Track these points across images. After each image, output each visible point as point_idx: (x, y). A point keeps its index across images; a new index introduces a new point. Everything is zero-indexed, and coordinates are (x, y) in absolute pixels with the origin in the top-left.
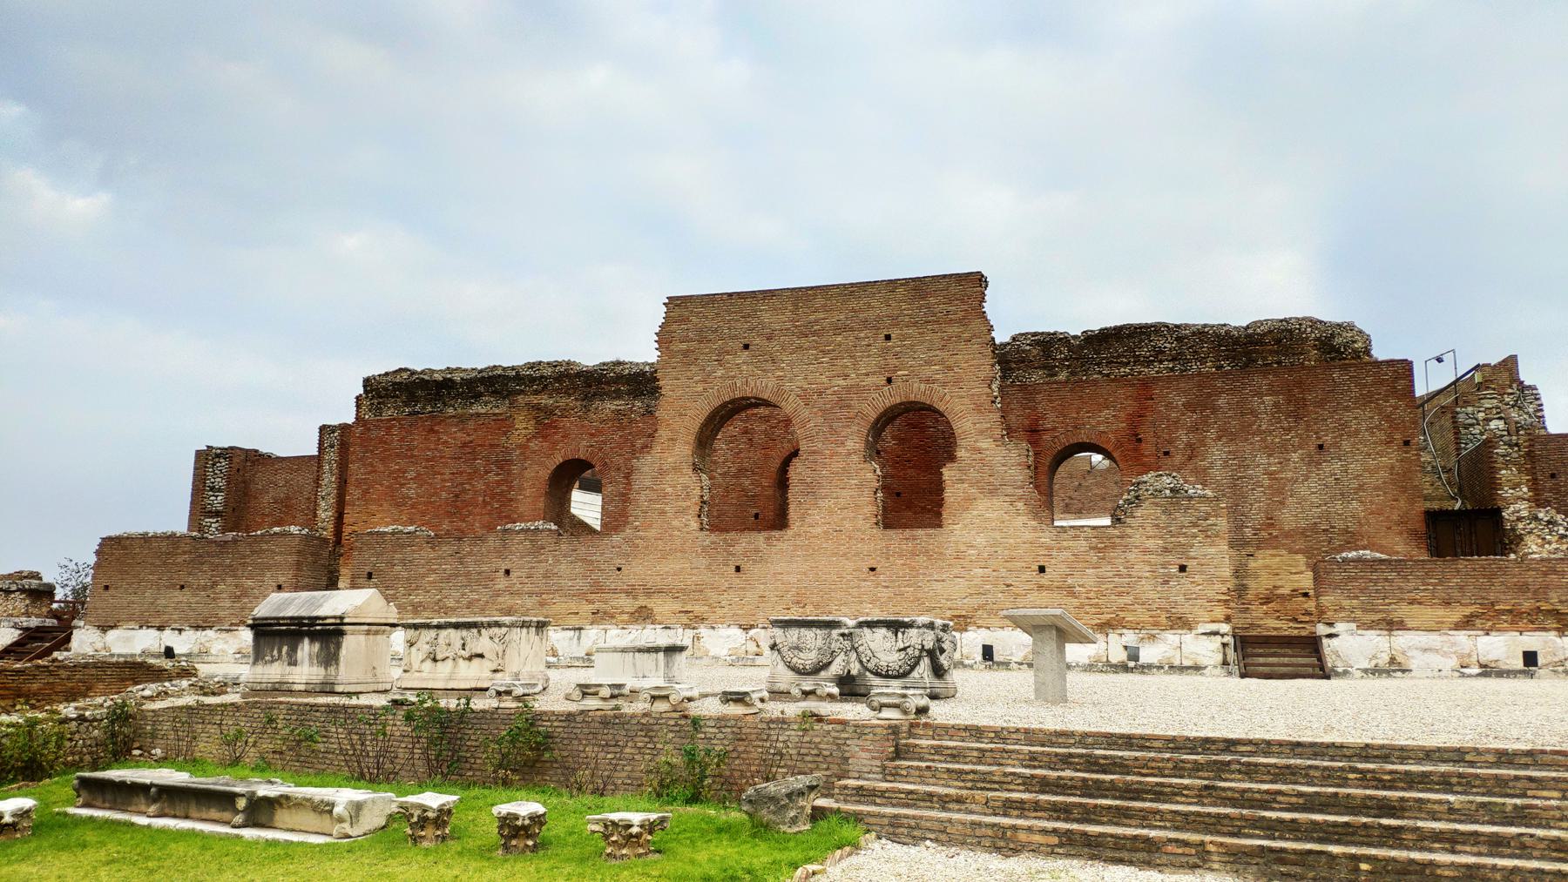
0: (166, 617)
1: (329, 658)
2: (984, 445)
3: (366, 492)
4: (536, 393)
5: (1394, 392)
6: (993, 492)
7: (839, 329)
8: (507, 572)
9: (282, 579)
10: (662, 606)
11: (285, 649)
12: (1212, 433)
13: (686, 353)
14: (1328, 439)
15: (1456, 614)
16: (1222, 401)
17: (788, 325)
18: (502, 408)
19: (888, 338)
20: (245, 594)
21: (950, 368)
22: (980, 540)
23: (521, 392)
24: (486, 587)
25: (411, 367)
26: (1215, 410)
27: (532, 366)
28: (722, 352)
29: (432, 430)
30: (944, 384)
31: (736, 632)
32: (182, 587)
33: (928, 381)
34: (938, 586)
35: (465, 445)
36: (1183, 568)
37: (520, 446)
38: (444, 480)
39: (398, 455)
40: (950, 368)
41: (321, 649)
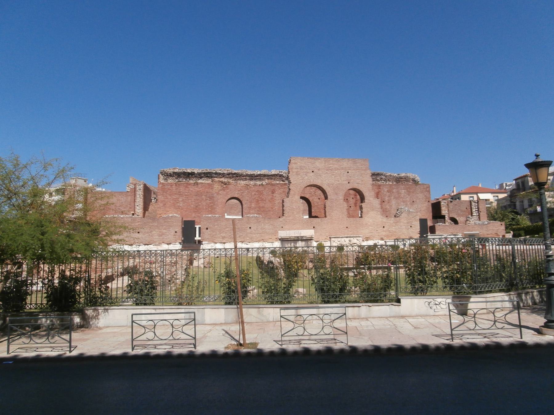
3: (165, 204)
4: (221, 178)
5: (426, 191)
6: (373, 210)
12: (392, 198)
13: (297, 172)
14: (414, 200)
16: (394, 191)
18: (209, 181)
20: (163, 234)
22: (371, 221)
23: (216, 177)
28: (307, 173)
29: (187, 187)
30: (362, 184)
35: (198, 191)
39: (176, 194)
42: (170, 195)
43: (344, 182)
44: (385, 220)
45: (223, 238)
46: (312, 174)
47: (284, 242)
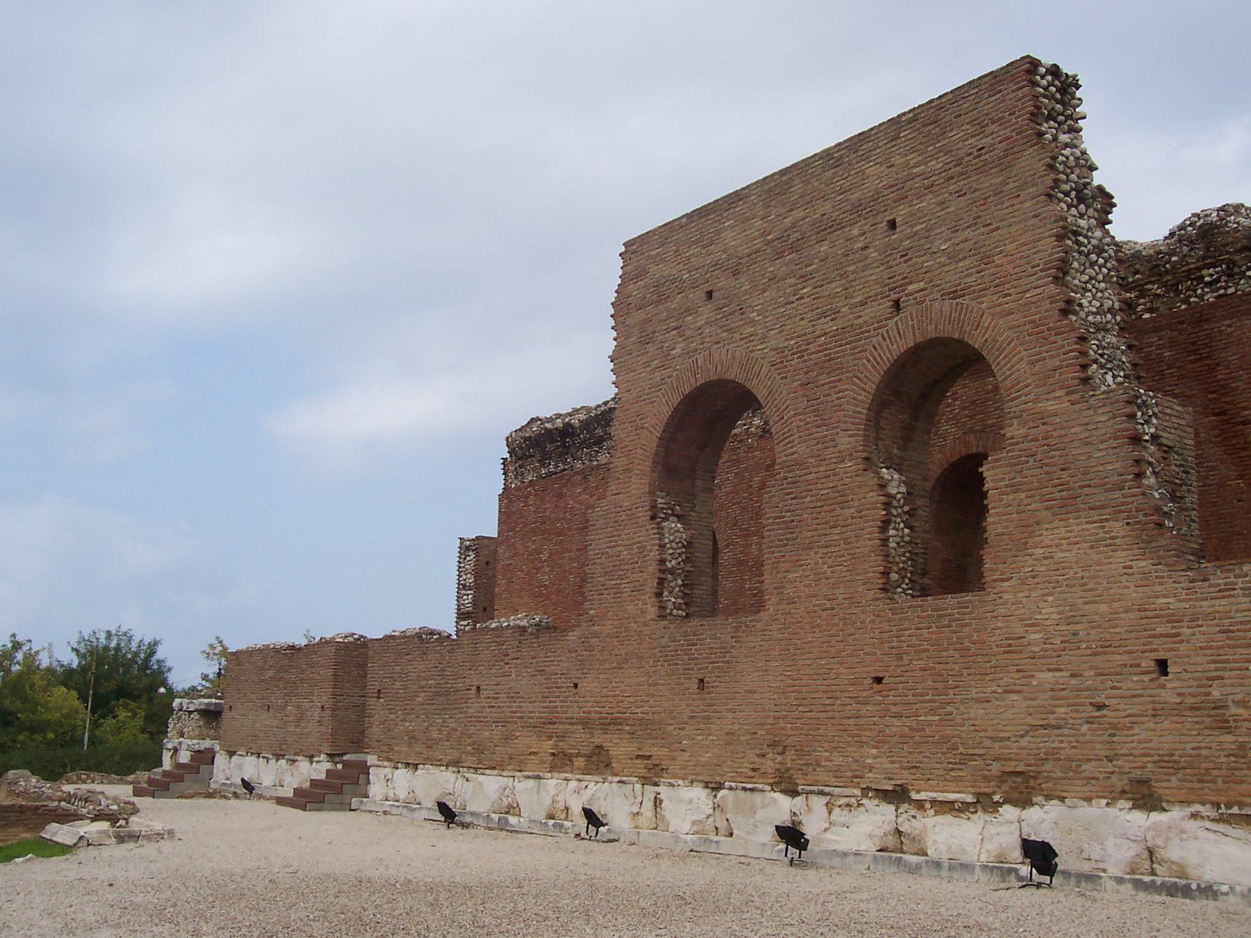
2: (1051, 406)
6: (1067, 505)
10: (620, 748)
19: (892, 225)
25: (542, 416)
31: (698, 793)
33: (954, 295)
34: (978, 711)
38: (571, 559)
43: (869, 312)
44: (1172, 592)
46: (707, 312)
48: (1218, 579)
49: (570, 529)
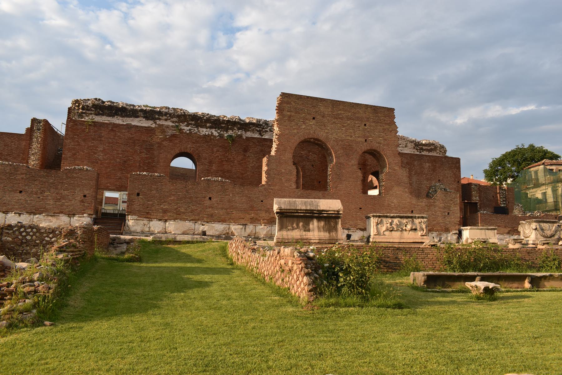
0: (10, 207)
1: (331, 229)
2: (396, 168)
3: (74, 154)
7: (349, 119)
8: (210, 198)
9: (86, 192)
11: (301, 224)
13: (290, 116)
15: (507, 231)
16: (416, 163)
17: (330, 113)
19: (365, 125)
20: (63, 198)
21: (386, 140)
23: (160, 119)
24: (199, 204)
26: (414, 166)
27: (162, 108)
29: (112, 130)
30: (384, 145)
32: (21, 192)
33: (379, 143)
36: (448, 213)
37: (158, 143)
39: (93, 139)
40: (386, 140)
41: (326, 224)
42: (84, 140)
43: (359, 139)
44: (414, 201)
45: (165, 211)
47: (285, 220)
48: (421, 200)
49: (117, 143)
